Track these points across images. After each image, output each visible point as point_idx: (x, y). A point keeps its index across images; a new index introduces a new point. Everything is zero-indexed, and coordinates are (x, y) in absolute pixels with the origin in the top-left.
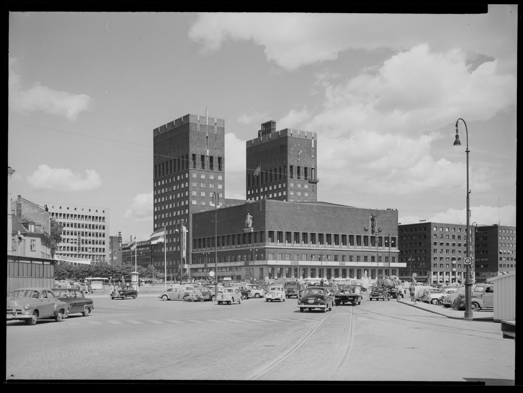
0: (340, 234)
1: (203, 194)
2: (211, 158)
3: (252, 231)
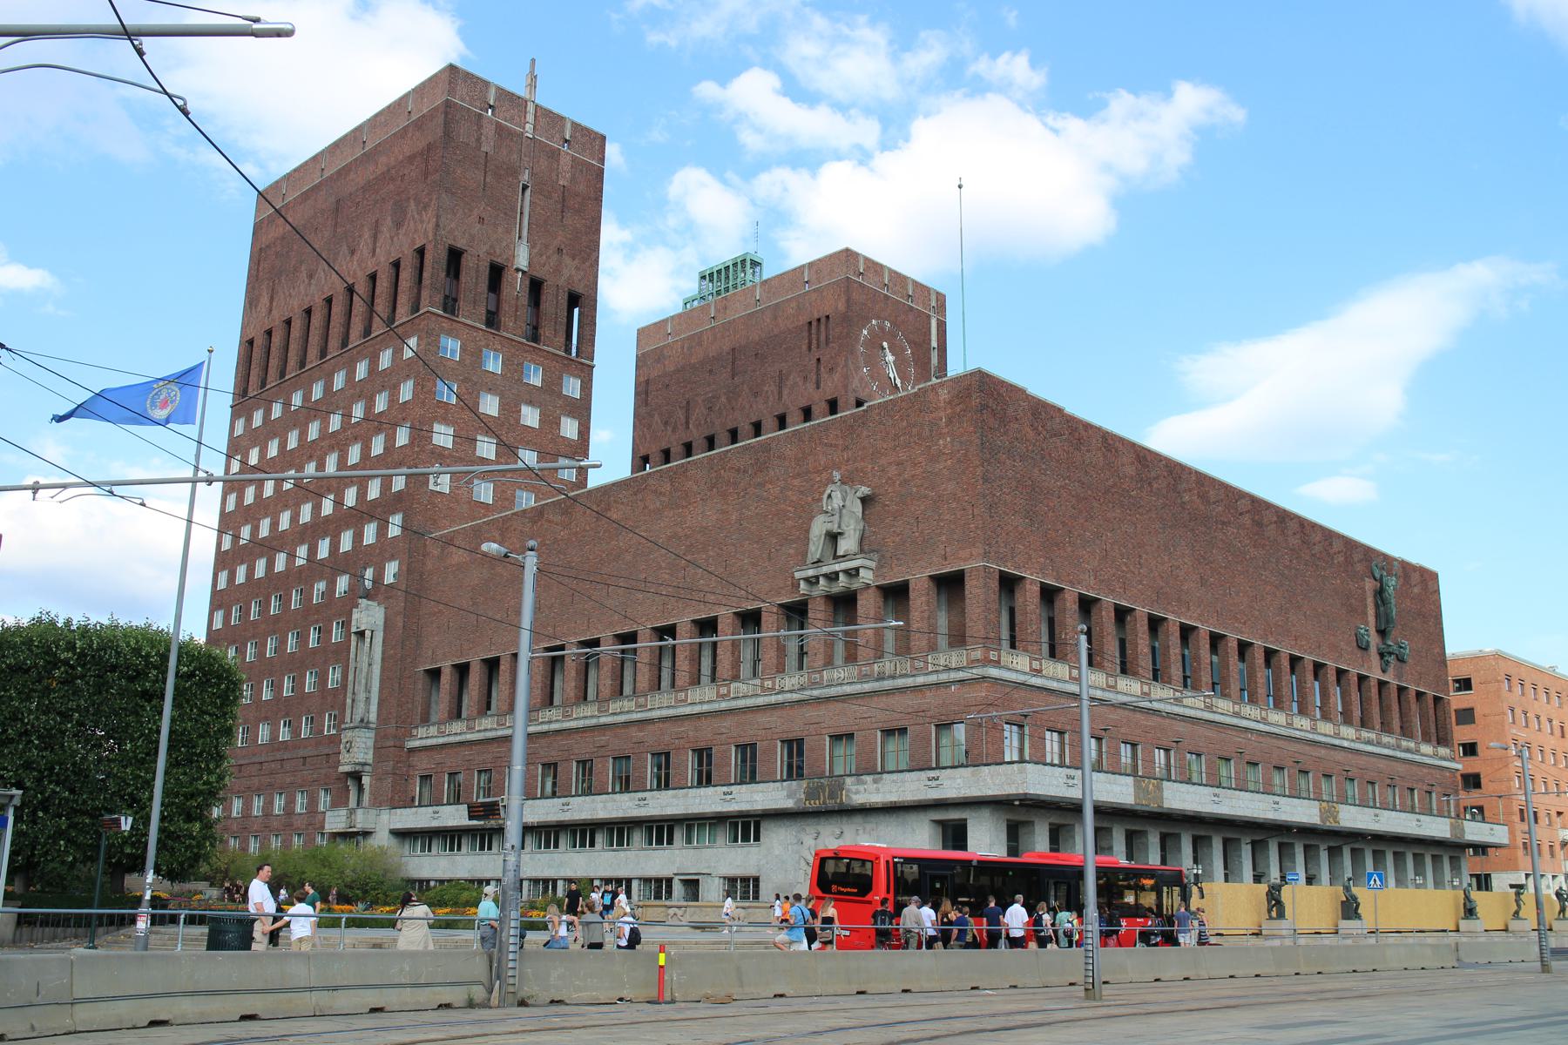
0: (1286, 650)
2: (536, 286)
3: (866, 576)
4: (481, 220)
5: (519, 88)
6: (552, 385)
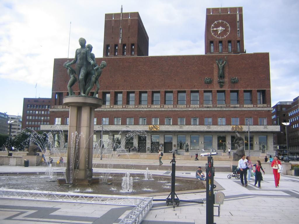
2: (124, 45)
4: (112, 38)
5: (119, 12)
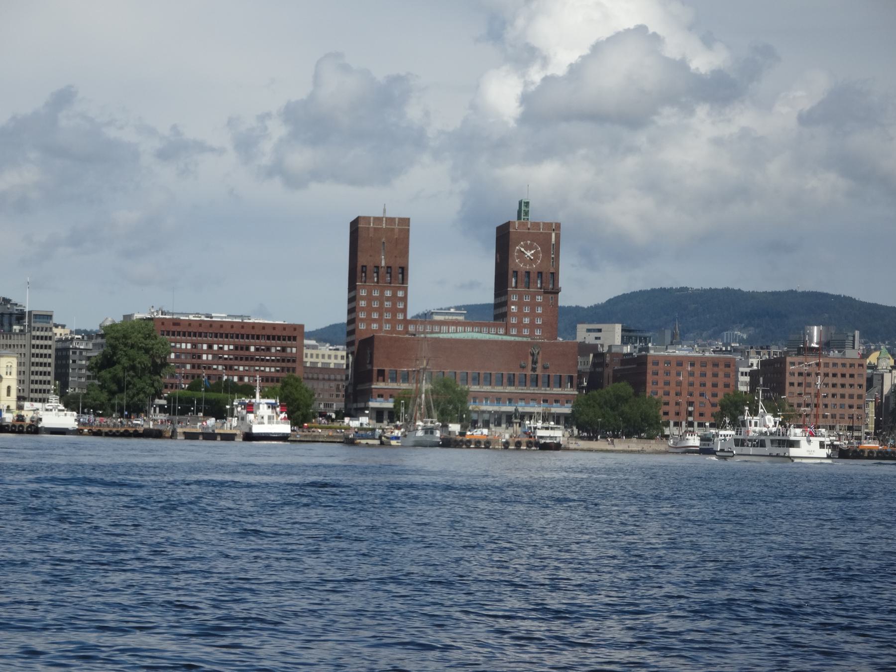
1: (375, 316)
5: (381, 215)
6: (394, 295)
